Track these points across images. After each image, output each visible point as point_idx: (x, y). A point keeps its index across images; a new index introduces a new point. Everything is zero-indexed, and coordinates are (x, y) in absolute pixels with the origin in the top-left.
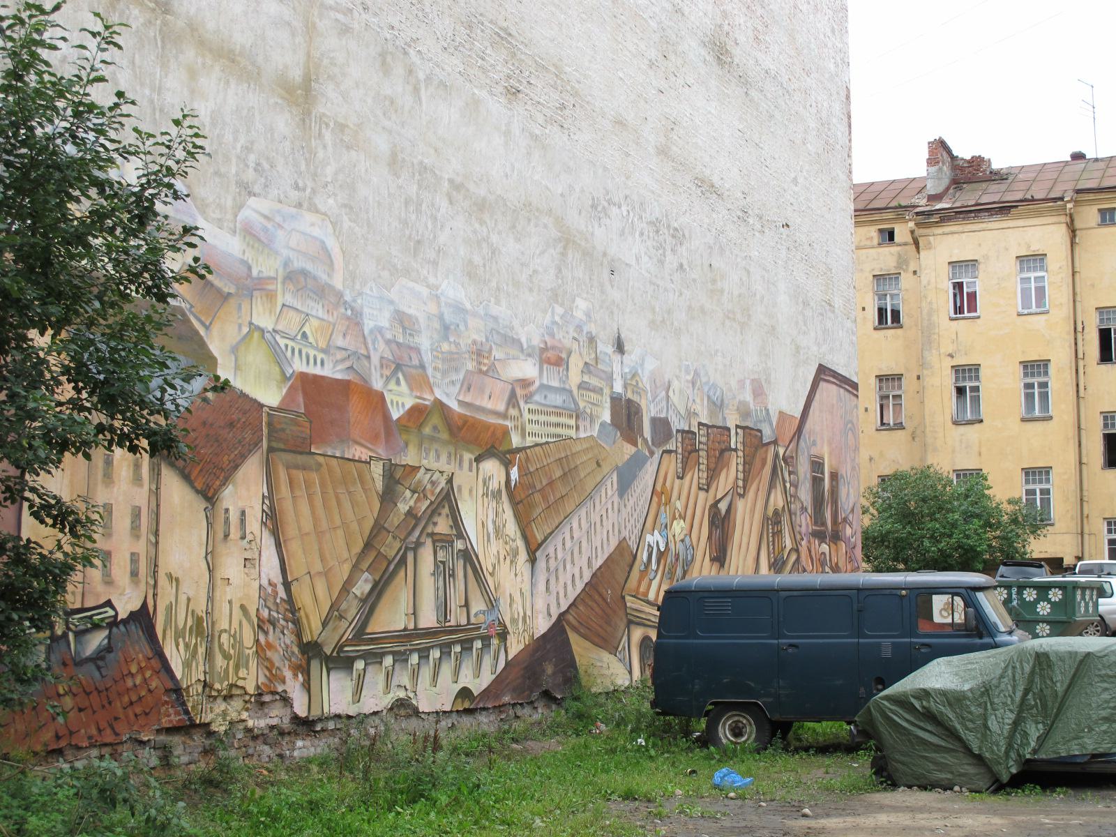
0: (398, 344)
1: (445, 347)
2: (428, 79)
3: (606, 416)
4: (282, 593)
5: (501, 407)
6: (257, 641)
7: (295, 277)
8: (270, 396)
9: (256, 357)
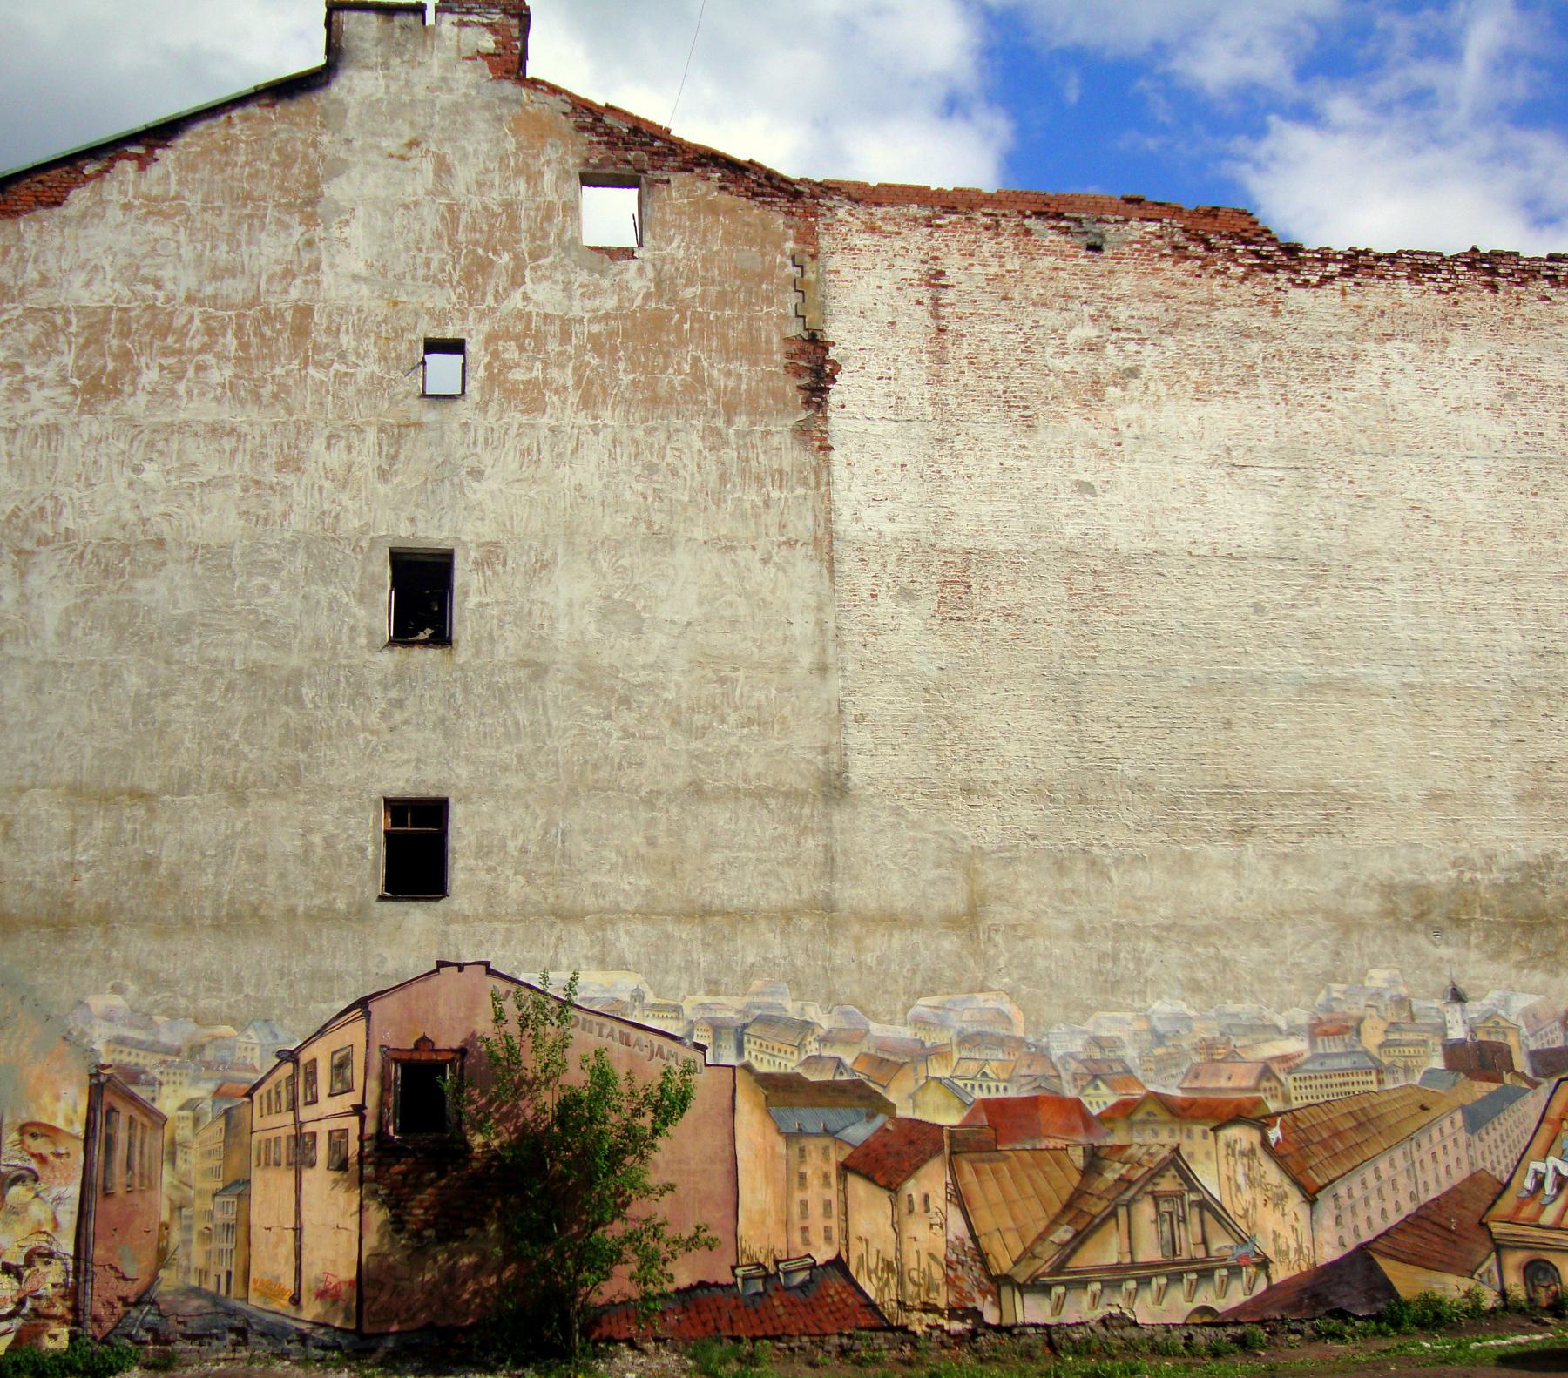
0: (1096, 1061)
1: (1159, 1051)
2: (1118, 861)
3: (1438, 1063)
4: (969, 1243)
5: (1250, 1083)
6: (947, 1276)
7: (965, 1040)
8: (950, 1118)
9: (934, 1096)
